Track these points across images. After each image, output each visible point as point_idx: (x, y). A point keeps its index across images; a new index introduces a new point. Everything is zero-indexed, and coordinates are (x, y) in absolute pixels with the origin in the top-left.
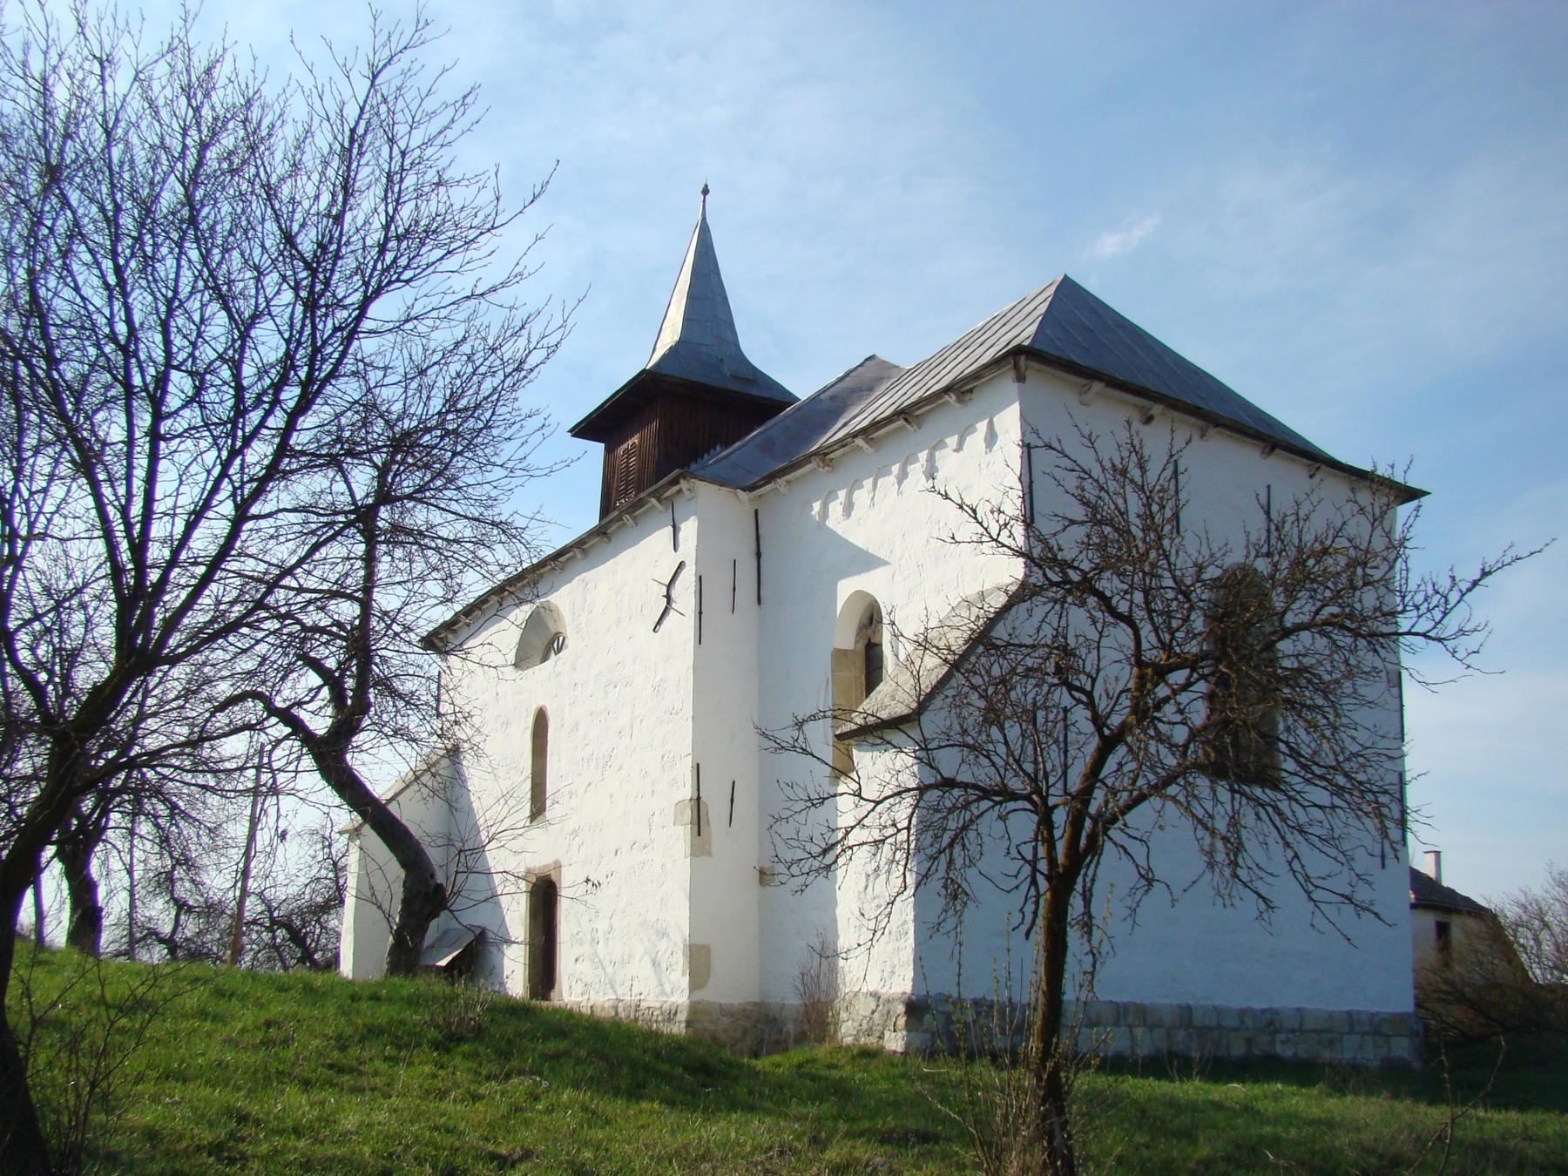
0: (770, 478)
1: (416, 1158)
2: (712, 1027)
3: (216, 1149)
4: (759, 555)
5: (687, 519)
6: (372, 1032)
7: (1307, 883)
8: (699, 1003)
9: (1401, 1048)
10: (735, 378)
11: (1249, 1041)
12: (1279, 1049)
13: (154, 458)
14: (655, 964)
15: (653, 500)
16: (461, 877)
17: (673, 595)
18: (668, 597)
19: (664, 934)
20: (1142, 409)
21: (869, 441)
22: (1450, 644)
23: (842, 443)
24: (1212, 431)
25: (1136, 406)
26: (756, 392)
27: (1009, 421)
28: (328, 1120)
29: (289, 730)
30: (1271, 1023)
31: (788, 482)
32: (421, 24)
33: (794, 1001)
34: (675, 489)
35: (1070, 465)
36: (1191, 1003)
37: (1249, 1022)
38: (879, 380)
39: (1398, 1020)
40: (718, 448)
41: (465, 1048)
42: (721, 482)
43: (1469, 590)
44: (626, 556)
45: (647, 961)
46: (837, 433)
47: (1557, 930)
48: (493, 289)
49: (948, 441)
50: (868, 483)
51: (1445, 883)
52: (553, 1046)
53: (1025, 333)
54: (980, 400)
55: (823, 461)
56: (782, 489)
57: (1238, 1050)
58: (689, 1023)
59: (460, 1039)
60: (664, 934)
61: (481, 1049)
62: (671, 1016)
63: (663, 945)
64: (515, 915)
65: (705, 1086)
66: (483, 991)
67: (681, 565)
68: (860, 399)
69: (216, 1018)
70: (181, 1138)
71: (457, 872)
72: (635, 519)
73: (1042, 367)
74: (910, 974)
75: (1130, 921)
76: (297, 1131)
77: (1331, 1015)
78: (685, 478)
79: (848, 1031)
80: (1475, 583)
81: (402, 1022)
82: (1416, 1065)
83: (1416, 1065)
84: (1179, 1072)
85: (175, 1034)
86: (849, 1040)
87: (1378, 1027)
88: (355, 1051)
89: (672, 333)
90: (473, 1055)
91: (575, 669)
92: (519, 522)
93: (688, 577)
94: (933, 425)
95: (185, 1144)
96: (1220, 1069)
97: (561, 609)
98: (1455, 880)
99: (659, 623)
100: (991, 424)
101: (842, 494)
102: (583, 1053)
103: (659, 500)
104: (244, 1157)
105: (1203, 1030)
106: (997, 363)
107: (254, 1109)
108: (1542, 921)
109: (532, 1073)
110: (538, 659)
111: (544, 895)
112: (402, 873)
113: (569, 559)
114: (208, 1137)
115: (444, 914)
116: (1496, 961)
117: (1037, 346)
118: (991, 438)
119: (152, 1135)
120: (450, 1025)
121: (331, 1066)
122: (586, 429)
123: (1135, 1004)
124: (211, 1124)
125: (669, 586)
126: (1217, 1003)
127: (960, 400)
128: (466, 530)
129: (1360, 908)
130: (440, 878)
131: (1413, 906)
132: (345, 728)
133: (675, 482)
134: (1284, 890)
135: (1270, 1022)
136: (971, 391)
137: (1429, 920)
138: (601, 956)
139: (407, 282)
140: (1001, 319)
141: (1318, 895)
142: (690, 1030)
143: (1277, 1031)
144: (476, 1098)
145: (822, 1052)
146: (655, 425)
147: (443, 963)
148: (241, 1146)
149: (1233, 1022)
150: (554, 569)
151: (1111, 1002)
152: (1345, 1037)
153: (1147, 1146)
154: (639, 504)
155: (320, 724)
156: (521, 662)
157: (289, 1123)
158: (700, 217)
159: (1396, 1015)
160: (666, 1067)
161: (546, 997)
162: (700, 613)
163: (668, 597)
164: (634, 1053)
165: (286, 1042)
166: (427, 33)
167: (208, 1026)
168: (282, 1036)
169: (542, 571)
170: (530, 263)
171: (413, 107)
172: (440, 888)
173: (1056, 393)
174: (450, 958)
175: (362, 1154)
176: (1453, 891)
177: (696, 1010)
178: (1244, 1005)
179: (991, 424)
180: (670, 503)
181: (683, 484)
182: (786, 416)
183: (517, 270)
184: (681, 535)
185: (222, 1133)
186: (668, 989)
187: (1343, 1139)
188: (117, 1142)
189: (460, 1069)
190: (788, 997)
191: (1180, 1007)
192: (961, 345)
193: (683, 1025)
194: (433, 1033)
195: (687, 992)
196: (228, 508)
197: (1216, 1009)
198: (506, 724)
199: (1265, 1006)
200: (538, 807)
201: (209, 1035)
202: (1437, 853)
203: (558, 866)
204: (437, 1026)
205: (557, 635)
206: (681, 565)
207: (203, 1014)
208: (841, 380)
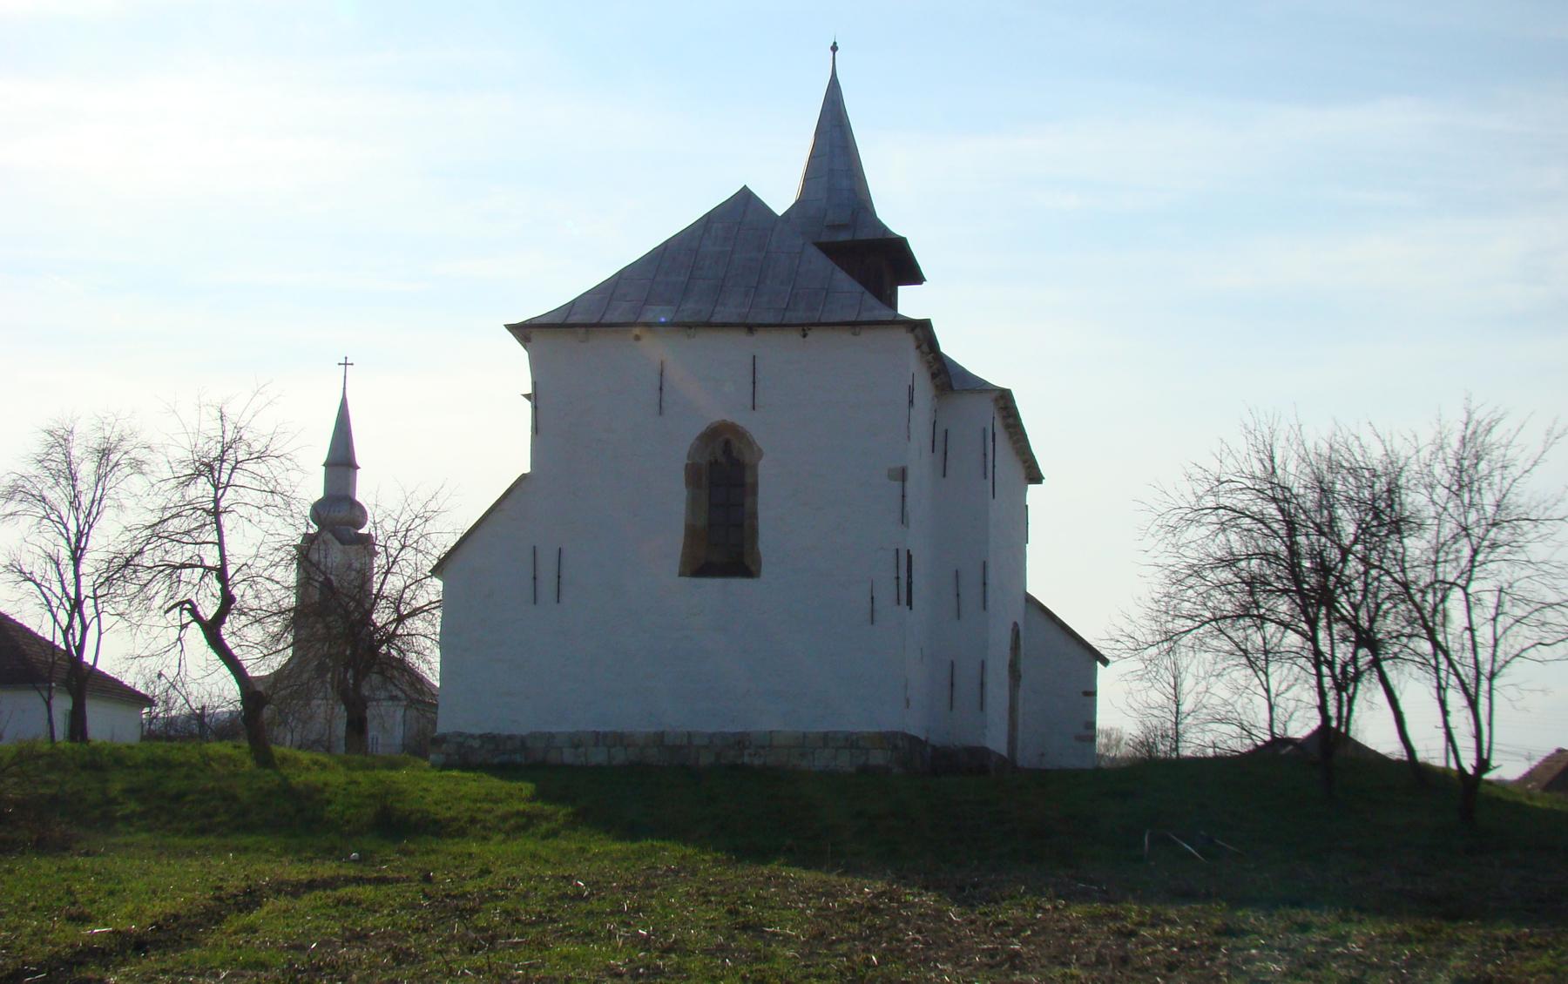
30: (739, 742)
77: (805, 735)
135: (741, 741)
151: (594, 731)
197: (689, 734)
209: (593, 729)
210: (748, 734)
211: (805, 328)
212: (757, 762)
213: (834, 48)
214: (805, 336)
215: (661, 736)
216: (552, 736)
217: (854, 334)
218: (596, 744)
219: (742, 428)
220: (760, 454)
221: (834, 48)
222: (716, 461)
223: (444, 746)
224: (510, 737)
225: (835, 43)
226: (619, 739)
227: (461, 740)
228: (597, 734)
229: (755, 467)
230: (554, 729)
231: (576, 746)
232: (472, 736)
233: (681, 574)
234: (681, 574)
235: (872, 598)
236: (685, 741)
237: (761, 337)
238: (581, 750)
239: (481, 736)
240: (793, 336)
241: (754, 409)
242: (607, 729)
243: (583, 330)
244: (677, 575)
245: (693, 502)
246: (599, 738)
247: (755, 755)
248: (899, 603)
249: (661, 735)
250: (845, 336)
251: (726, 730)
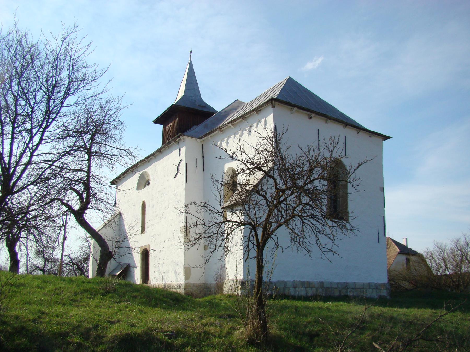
0: (206, 135)
1: (88, 322)
2: (191, 290)
3: (34, 320)
4: (203, 157)
5: (182, 147)
6: (85, 291)
7: (321, 247)
8: (187, 283)
9: (384, 293)
10: (199, 106)
11: (340, 291)
12: (349, 293)
13: (13, 139)
14: (175, 273)
15: (173, 142)
16: (117, 249)
17: (179, 168)
18: (178, 169)
19: (178, 264)
20: (308, 115)
21: (233, 125)
22: (352, 183)
23: (225, 125)
24: (329, 121)
25: (307, 114)
26: (205, 110)
27: (270, 119)
28: (66, 313)
29: (67, 209)
30: (346, 286)
31: (211, 136)
32: (76, 26)
33: (214, 282)
34: (179, 139)
35: (260, 136)
36: (323, 281)
37: (340, 286)
38: (239, 106)
39: (384, 285)
40: (195, 126)
41: (110, 295)
42: (192, 137)
43: (356, 169)
44: (166, 158)
45: (173, 272)
46: (226, 121)
47: (437, 259)
48: (99, 94)
49: (254, 124)
50: (233, 136)
51: (409, 247)
52: (135, 294)
53: (275, 94)
54: (263, 113)
55: (220, 130)
56: (209, 139)
57: (337, 294)
58: (185, 289)
59: (109, 292)
60: (178, 264)
61: (115, 295)
62: (180, 287)
63: (177, 267)
64: (137, 259)
65: (176, 304)
66: (129, 280)
67: (181, 160)
68: (234, 112)
69: (42, 288)
70: (25, 317)
71: (115, 248)
72: (168, 147)
73: (279, 104)
74: (242, 274)
75: (272, 257)
76: (57, 316)
77: (364, 284)
78: (182, 136)
79: (226, 290)
80: (358, 168)
81: (93, 288)
82: (388, 297)
83: (388, 297)
84: (314, 299)
85: (30, 293)
86: (226, 293)
87: (377, 287)
88: (79, 296)
89: (181, 94)
90: (112, 297)
91: (153, 190)
92: (131, 149)
93: (183, 164)
94: (250, 120)
95: (26, 319)
96: (326, 299)
97: (149, 172)
98: (412, 246)
99: (175, 177)
100: (265, 120)
101: (226, 140)
102: (142, 296)
103: (175, 142)
104: (41, 322)
105: (327, 289)
106: (267, 102)
107: (47, 311)
108: (433, 257)
109: (127, 301)
110: (143, 186)
111: (145, 254)
112: (100, 248)
113: (151, 159)
114: (31, 317)
115: (112, 259)
116: (420, 269)
117: (280, 98)
118: (266, 124)
119: (17, 317)
120: (107, 289)
121: (72, 300)
122: (157, 121)
123: (307, 281)
124: (34, 314)
125: (178, 166)
126: (331, 281)
127: (257, 113)
128: (115, 152)
129: (334, 252)
130: (110, 249)
131: (399, 253)
132: (84, 207)
133: (179, 137)
134: (315, 249)
135: (346, 286)
136: (260, 110)
137: (403, 257)
138: (161, 271)
139: (72, 94)
140: (271, 89)
141: (323, 249)
142: (185, 291)
143: (348, 289)
144: (110, 307)
145: (218, 296)
146: (177, 120)
147: (117, 274)
148: (41, 320)
149: (336, 286)
150: (146, 162)
153: (294, 318)
154: (170, 143)
155: (76, 207)
156: (139, 187)
157: (55, 314)
158: (190, 60)
160: (165, 299)
161: (146, 283)
162: (187, 174)
163: (178, 169)
164: (157, 296)
165: (60, 294)
166: (78, 29)
167: (39, 290)
168: (59, 293)
169: (143, 162)
170: (108, 87)
171: (76, 47)
172: (110, 252)
173: (284, 111)
174: (120, 272)
175: (74, 321)
176: (411, 249)
177: (187, 286)
178: (339, 281)
179: (265, 120)
180: (178, 142)
181: (181, 137)
182: (215, 115)
183: (105, 89)
184: (181, 152)
185: (36, 316)
186: (179, 280)
187: (349, 317)
188: (8, 319)
189: (108, 300)
190: (212, 281)
191: (320, 282)
192: (260, 97)
193: (183, 290)
194: (102, 291)
195: (184, 280)
196: (29, 154)
198: (134, 206)
199: (345, 281)
200: (143, 229)
201: (39, 292)
202: (406, 238)
203: (149, 245)
204: (103, 289)
205: (148, 180)
206: (181, 160)
207: (38, 287)
208: (228, 107)
213: (191, 52)
214: (358, 133)
215: (322, 283)
216: (285, 283)
217: (370, 136)
221: (191, 52)
230: (286, 280)
231: (295, 287)
238: (297, 289)
246: (303, 284)
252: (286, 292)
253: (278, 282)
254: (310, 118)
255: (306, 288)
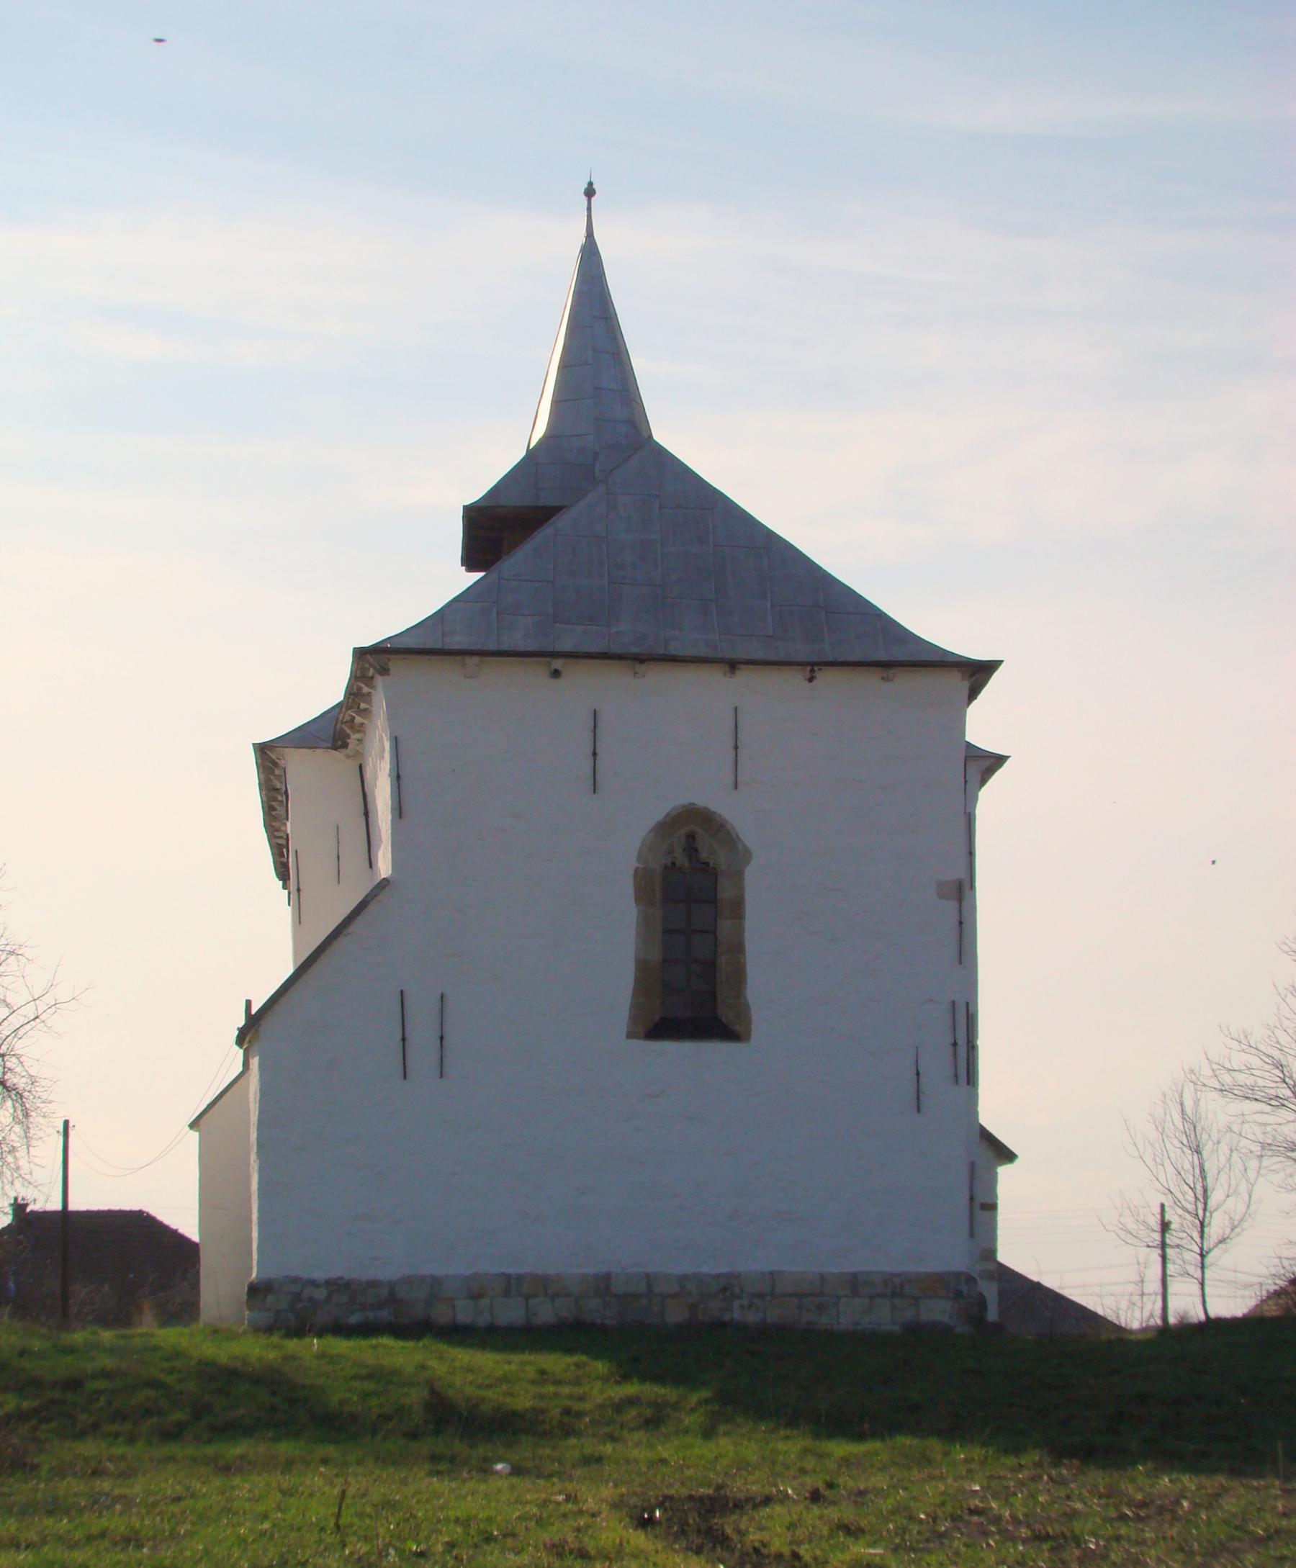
11: (693, 1307)
24: (639, 668)
30: (725, 1289)
77: (822, 1278)
126: (651, 1269)
135: (728, 1287)
151: (503, 1274)
152: (844, 1300)
159: (927, 1274)
209: (503, 1270)
210: (738, 1276)
211: (812, 668)
212: (753, 1318)
213: (590, 192)
214: (811, 680)
215: (602, 1285)
216: (435, 1282)
218: (507, 1293)
219: (720, 816)
220: (747, 856)
221: (590, 192)
222: (673, 864)
223: (270, 1298)
224: (373, 1284)
225: (591, 184)
226: (542, 1285)
227: (296, 1288)
228: (508, 1277)
229: (738, 876)
230: (440, 1271)
231: (476, 1296)
232: (313, 1283)
233: (630, 1035)
234: (630, 1035)
235: (918, 1074)
236: (642, 1287)
237: (745, 677)
238: (484, 1302)
239: (328, 1283)
240: (793, 681)
241: (736, 788)
242: (524, 1269)
243: (476, 659)
244: (624, 1035)
245: (645, 924)
246: (511, 1285)
247: (750, 1306)
248: (957, 1083)
249: (608, 1276)
250: (869, 681)
251: (705, 1269)
252: (441, 1314)
253: (408, 1281)
254: (556, 674)
255: (527, 1298)
